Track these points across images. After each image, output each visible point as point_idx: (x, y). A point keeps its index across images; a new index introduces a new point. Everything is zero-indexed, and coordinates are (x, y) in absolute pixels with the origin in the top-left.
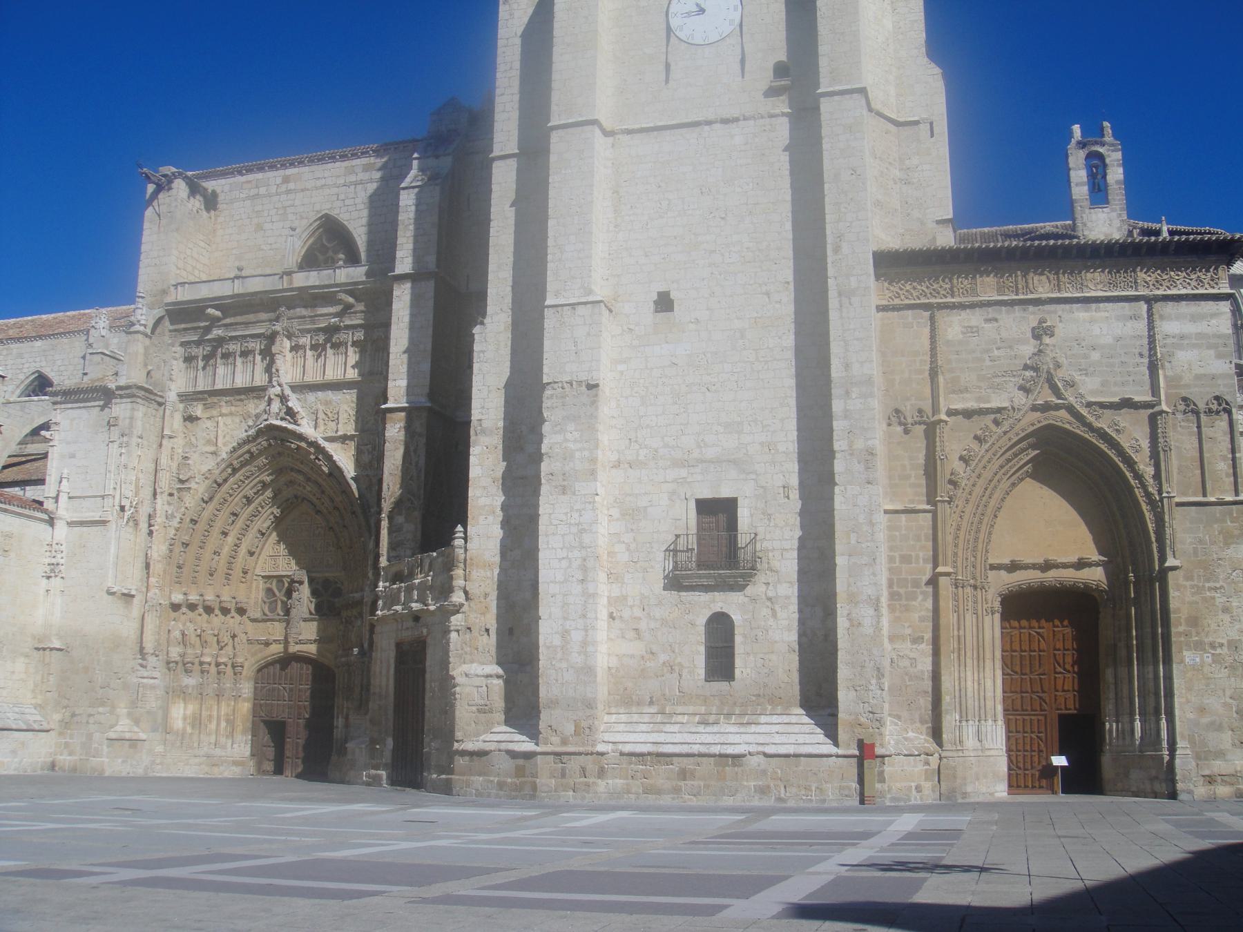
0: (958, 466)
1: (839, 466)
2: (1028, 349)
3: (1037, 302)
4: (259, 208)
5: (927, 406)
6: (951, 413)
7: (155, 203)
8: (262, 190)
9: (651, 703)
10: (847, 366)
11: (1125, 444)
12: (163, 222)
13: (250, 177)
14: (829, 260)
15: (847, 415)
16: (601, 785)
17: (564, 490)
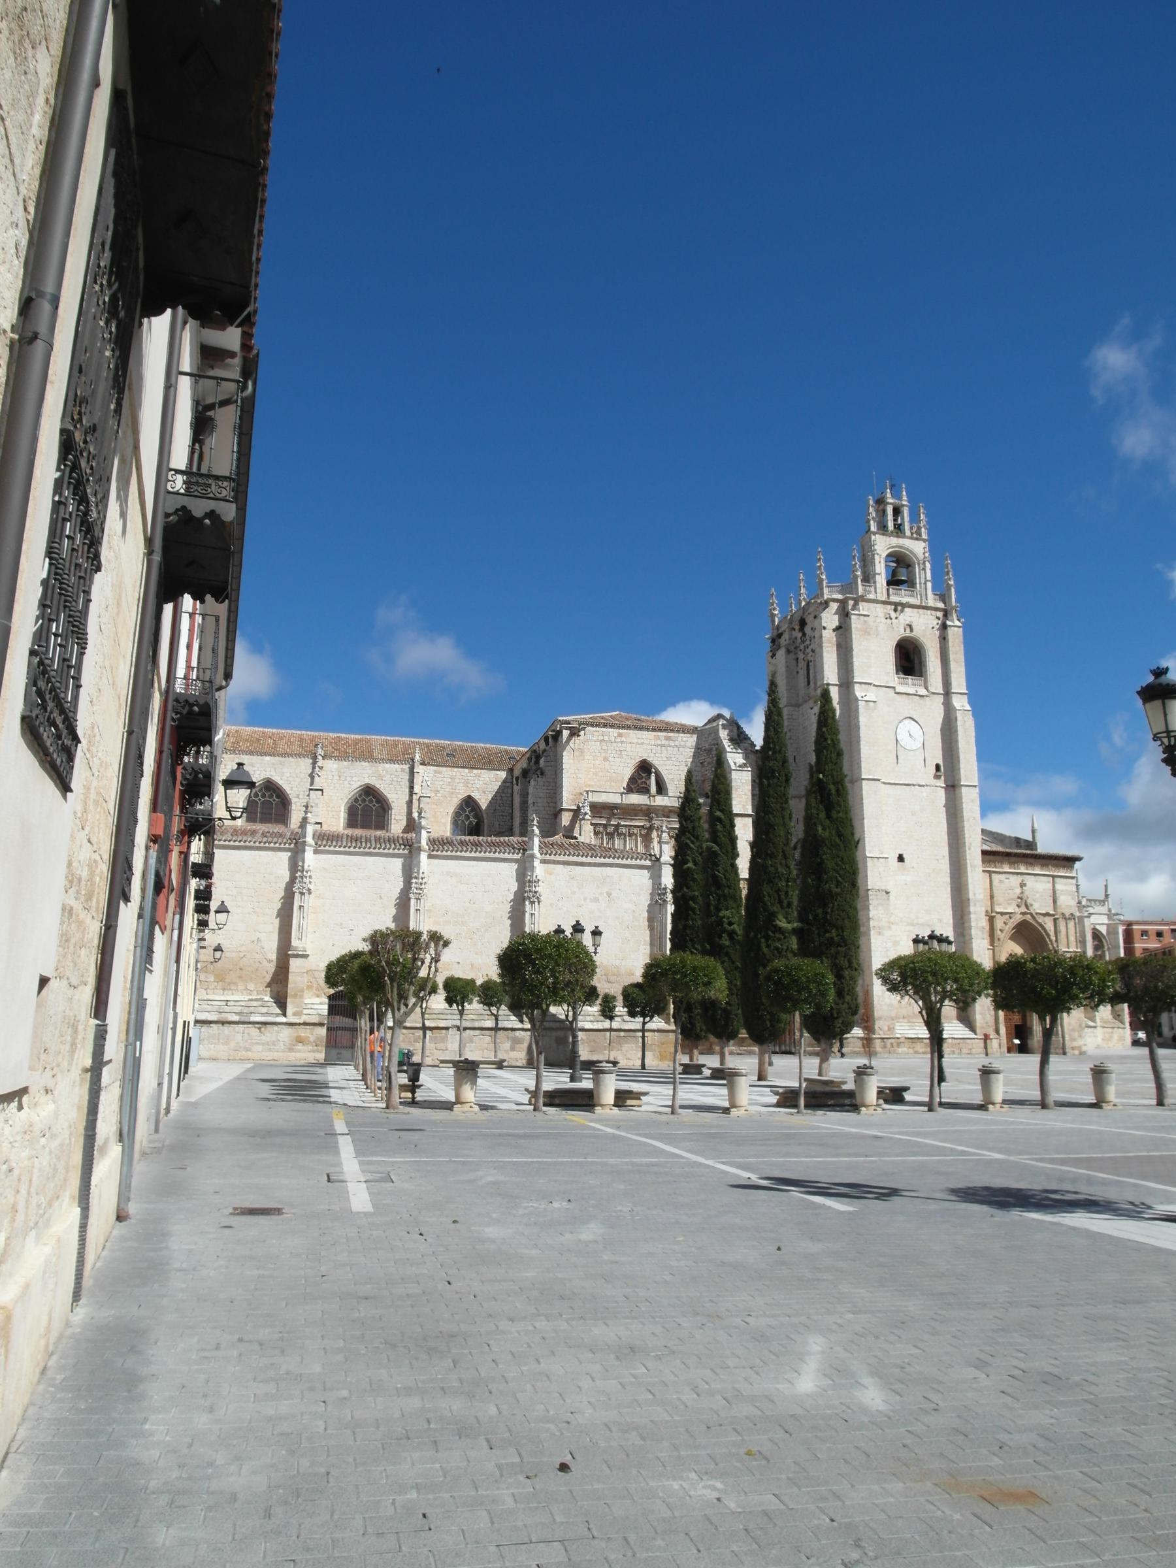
0: (999, 932)
1: (973, 932)
2: (1018, 891)
3: (1021, 874)
4: (605, 748)
5: (989, 909)
6: (997, 913)
7: (571, 744)
8: (606, 738)
9: (904, 1018)
10: (975, 894)
11: (1047, 928)
12: (576, 753)
13: (598, 729)
14: (968, 852)
15: (975, 913)
16: (900, 1050)
17: (879, 933)
